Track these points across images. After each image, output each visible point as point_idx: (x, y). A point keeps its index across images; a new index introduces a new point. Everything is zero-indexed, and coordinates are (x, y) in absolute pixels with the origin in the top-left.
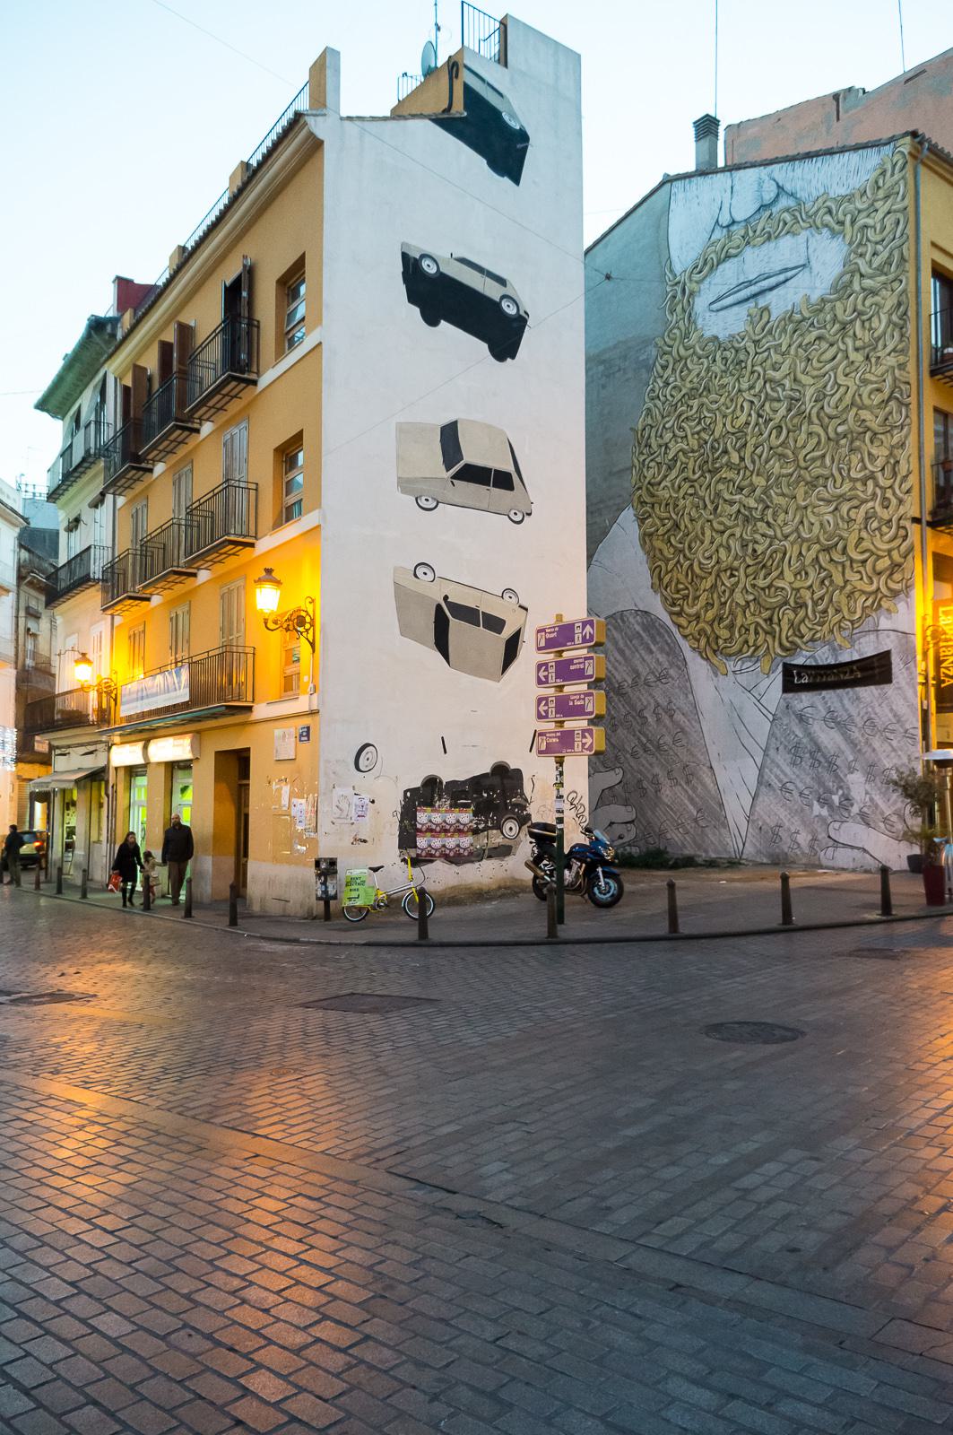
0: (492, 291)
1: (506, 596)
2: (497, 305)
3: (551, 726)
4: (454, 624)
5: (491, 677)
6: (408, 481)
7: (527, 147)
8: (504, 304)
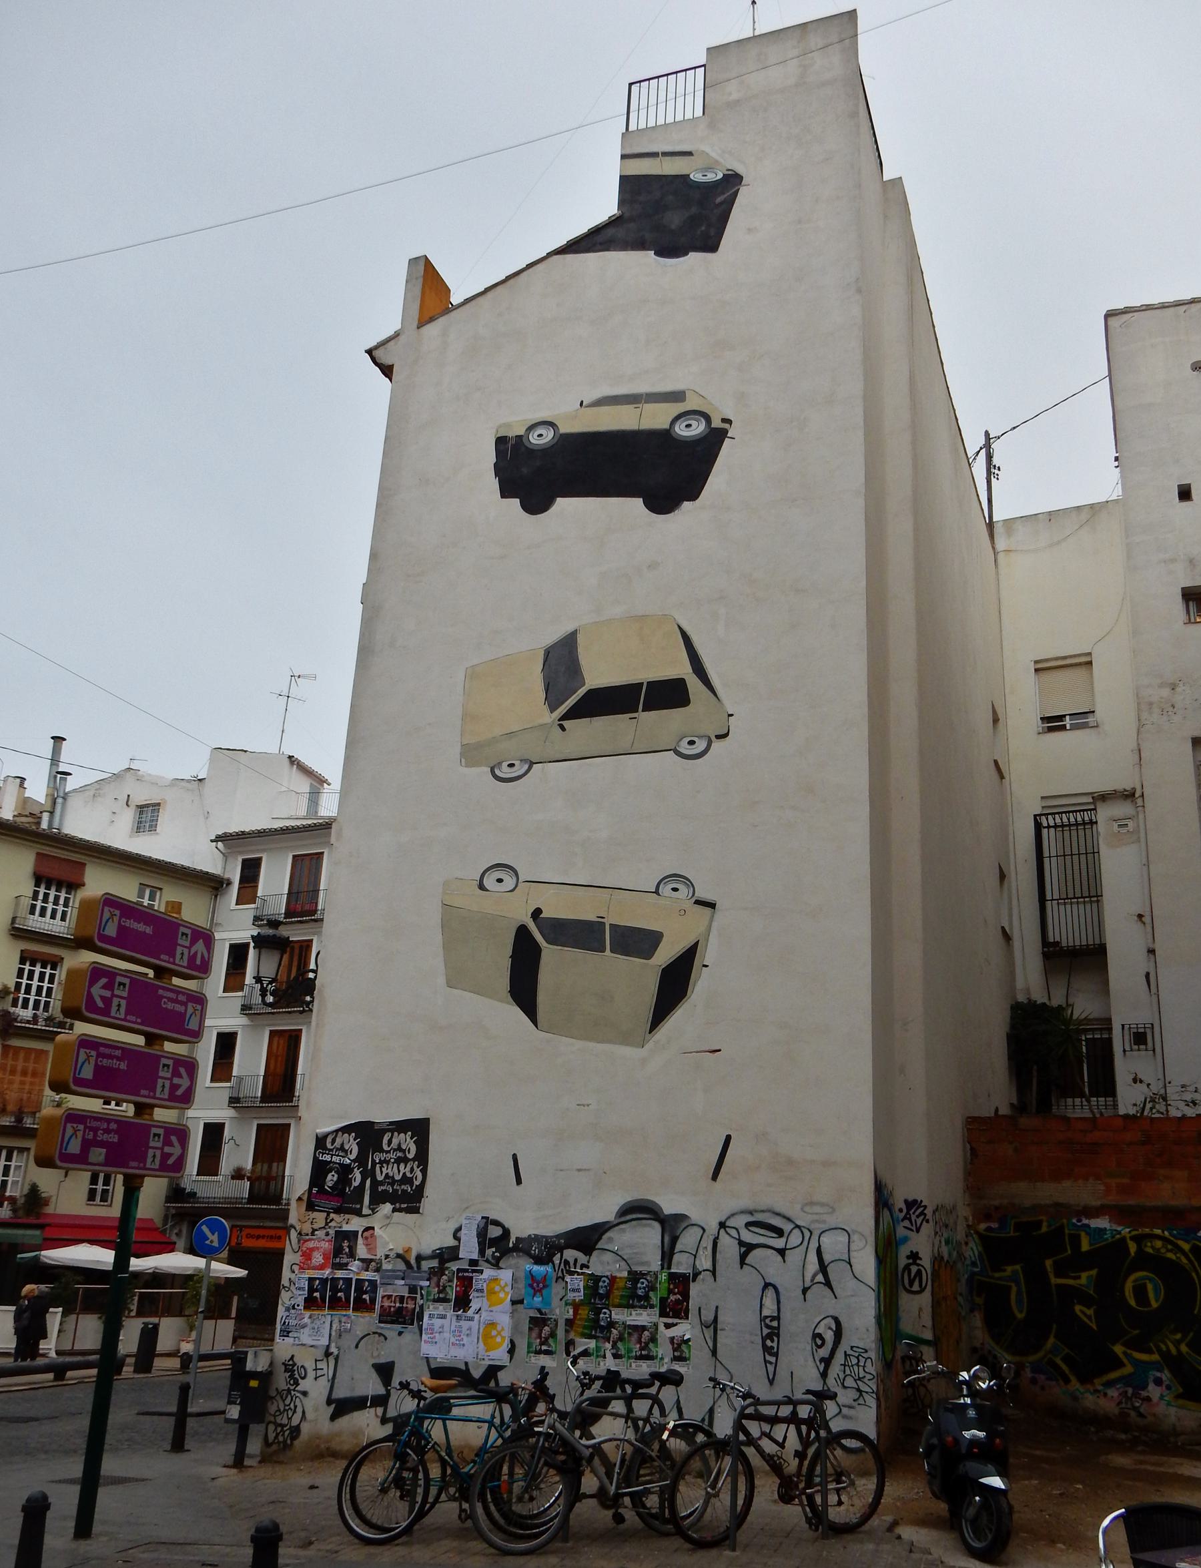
0: (656, 418)
1: (666, 890)
2: (664, 437)
3: (161, 1115)
4: (551, 955)
5: (626, 1039)
6: (479, 746)
7: (736, 194)
8: (681, 430)
